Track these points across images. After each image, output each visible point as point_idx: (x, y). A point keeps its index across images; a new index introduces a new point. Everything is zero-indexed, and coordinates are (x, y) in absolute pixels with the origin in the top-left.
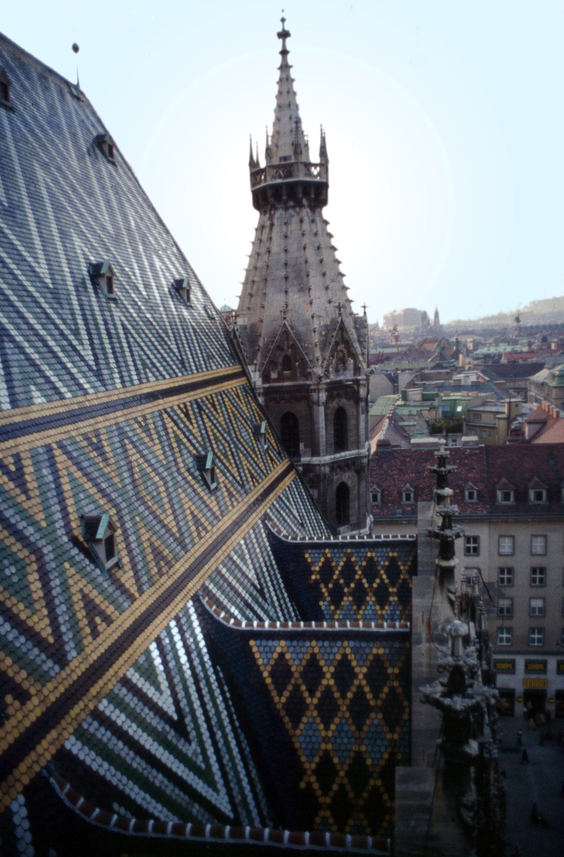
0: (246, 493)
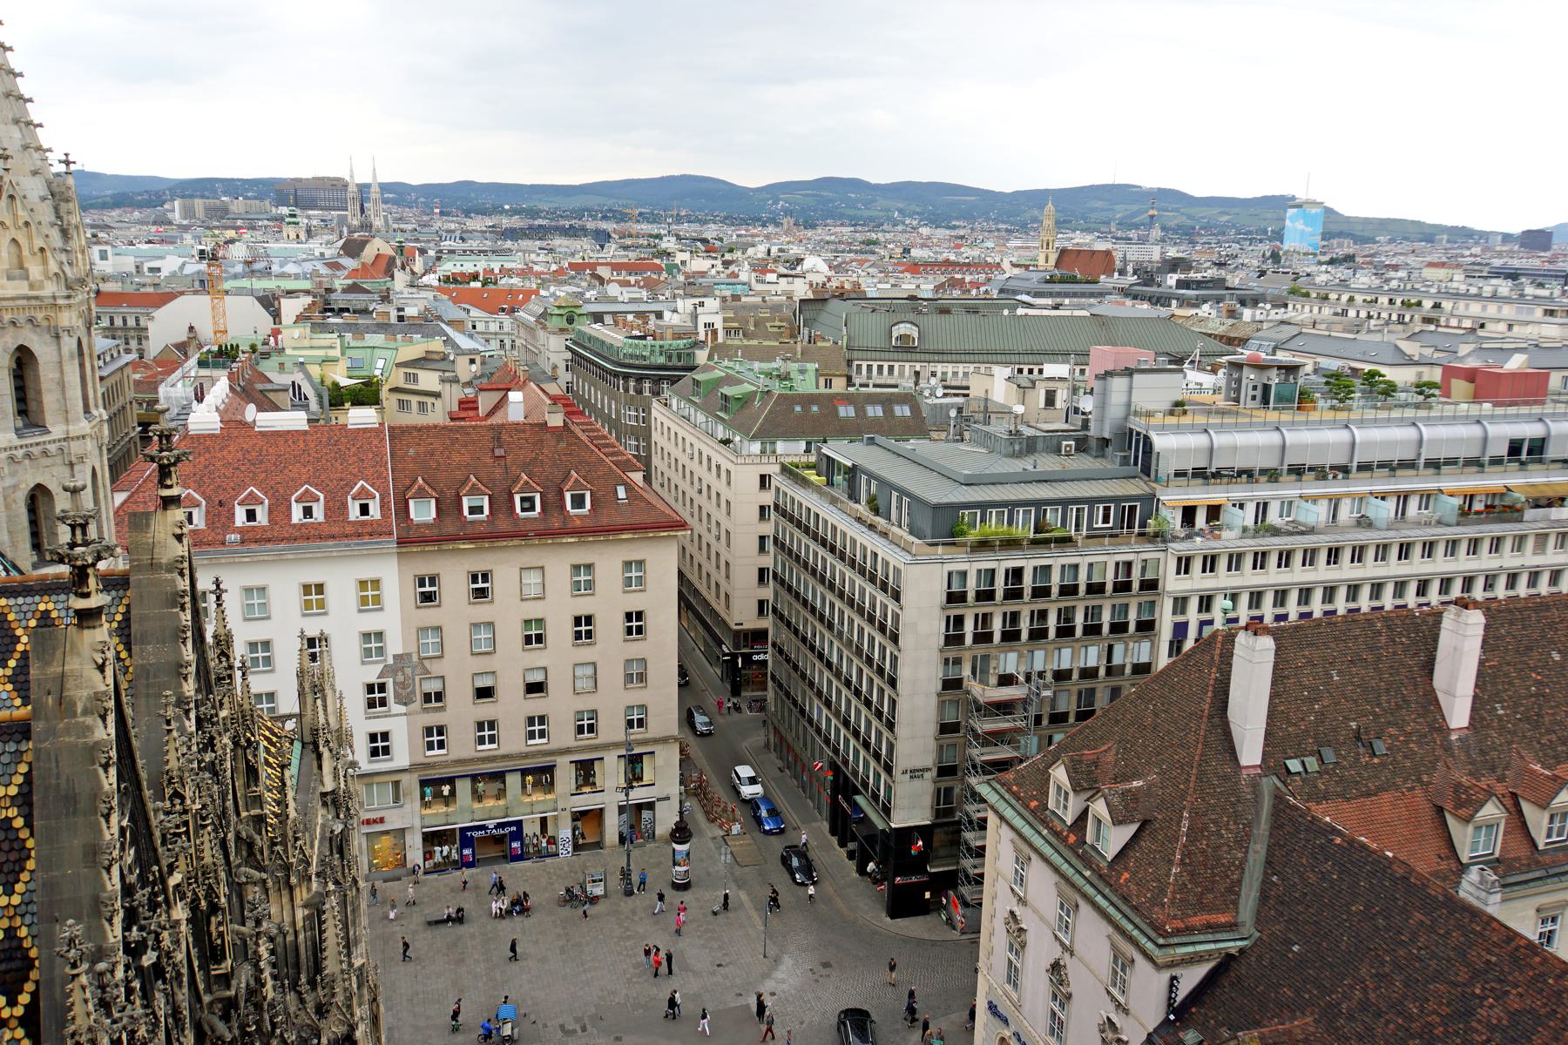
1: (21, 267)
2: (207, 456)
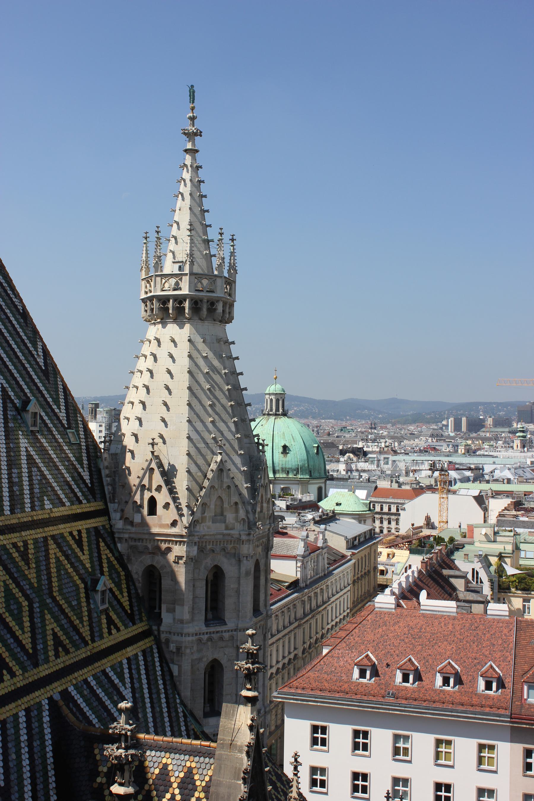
0: (36, 665)
1: (222, 514)
2: (384, 628)
